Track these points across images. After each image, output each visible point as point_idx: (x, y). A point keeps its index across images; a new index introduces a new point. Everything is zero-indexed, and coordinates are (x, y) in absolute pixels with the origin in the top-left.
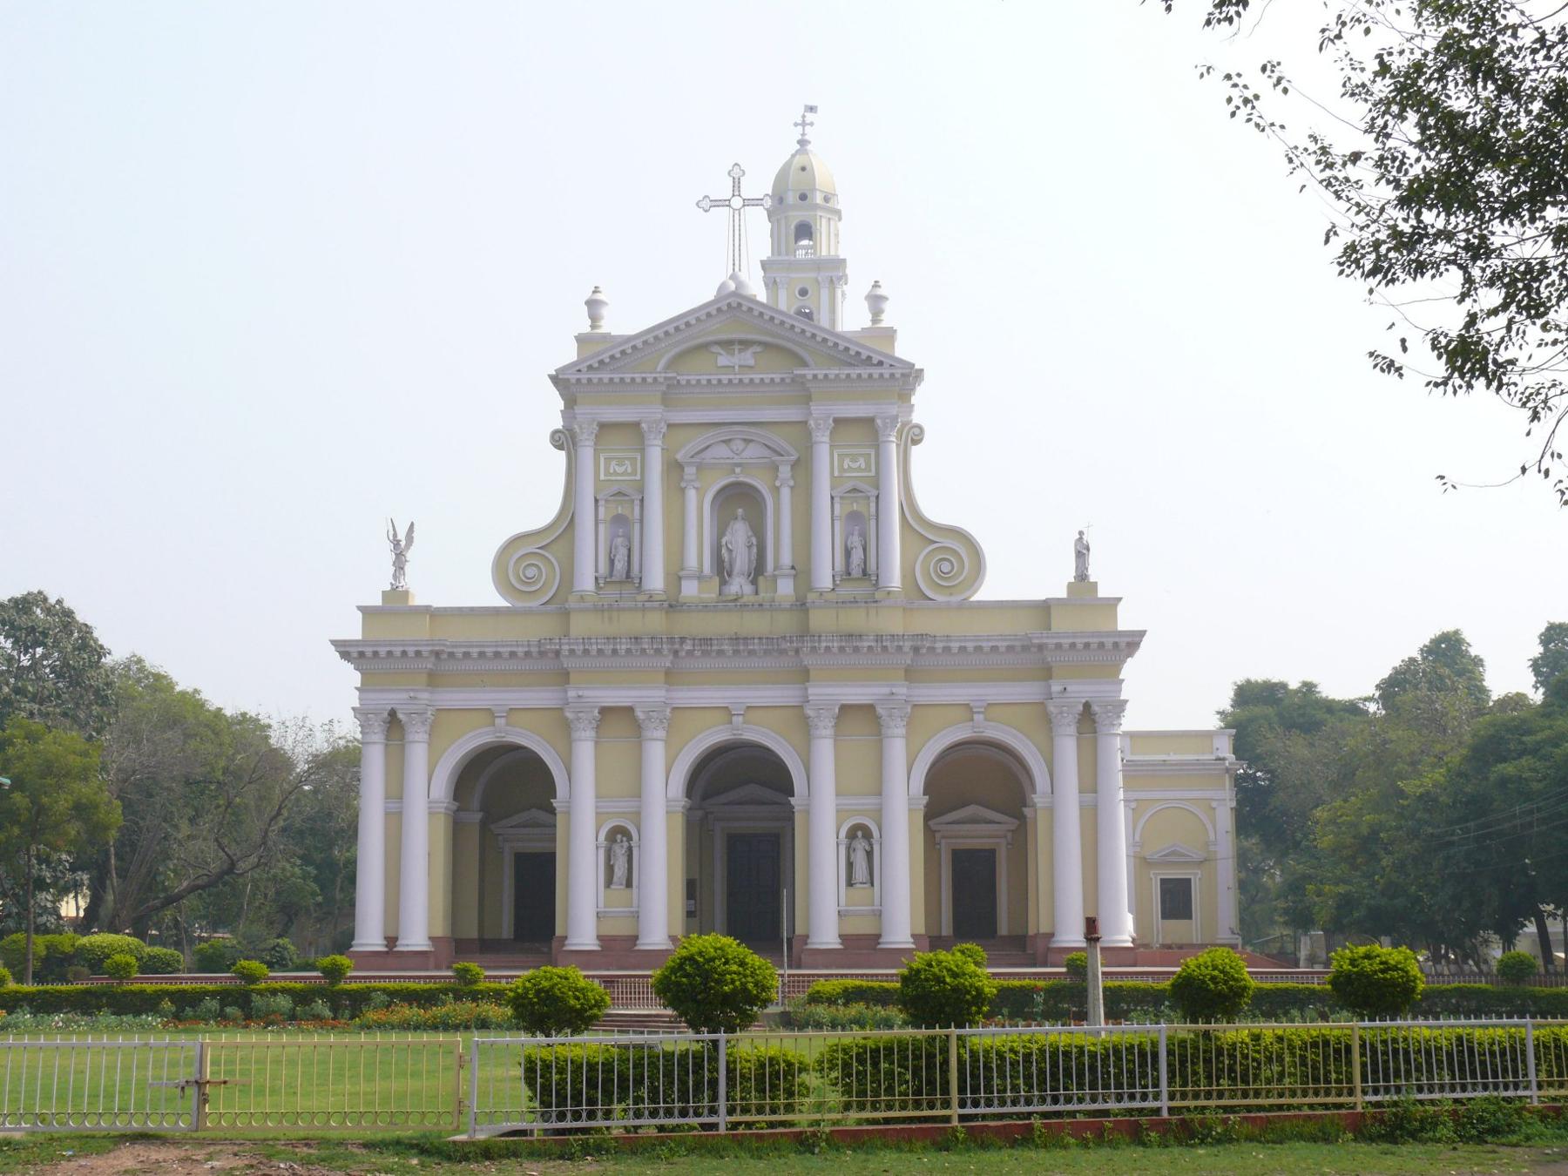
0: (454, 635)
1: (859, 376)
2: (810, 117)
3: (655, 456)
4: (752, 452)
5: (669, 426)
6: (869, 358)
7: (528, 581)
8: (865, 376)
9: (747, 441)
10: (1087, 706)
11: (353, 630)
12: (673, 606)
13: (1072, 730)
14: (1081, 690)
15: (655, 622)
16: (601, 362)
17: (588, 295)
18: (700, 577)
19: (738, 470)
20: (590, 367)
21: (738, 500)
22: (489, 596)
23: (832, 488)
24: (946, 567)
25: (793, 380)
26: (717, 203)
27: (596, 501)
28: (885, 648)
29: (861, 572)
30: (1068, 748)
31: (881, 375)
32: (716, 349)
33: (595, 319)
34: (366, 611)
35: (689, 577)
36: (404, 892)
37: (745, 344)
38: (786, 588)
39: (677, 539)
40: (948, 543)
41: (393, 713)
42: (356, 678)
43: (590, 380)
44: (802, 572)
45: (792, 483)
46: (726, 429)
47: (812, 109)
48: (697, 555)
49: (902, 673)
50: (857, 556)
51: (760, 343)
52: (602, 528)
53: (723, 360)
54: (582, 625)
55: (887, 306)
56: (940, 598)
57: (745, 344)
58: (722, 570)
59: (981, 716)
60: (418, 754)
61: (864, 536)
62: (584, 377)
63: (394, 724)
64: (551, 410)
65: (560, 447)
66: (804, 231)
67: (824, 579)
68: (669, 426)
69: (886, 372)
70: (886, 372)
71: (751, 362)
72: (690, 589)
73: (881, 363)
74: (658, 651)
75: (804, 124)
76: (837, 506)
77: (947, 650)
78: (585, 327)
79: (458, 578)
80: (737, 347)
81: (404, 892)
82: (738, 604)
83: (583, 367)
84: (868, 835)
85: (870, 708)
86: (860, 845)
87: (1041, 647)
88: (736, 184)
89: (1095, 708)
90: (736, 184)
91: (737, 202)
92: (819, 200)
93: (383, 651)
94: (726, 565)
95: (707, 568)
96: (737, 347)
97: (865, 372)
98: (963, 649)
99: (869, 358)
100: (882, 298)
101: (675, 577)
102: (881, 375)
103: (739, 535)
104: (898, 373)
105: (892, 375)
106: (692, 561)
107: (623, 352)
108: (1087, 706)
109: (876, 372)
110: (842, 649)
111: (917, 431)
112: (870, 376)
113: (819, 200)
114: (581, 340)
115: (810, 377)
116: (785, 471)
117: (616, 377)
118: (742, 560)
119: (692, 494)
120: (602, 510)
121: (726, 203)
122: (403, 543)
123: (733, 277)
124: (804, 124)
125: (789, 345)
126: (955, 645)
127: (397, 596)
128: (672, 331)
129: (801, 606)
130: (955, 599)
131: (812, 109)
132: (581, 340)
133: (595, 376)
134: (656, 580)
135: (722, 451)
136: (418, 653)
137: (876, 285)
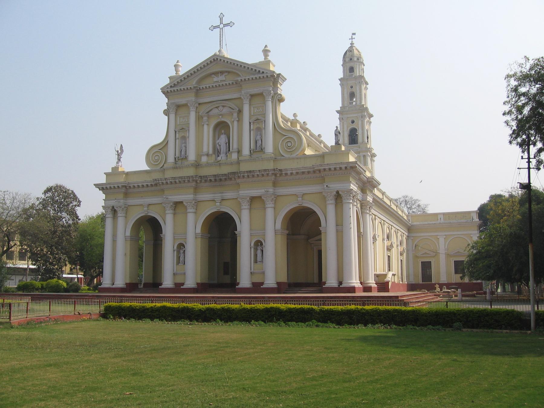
0: (133, 180)
1: (256, 78)
2: (354, 36)
3: (193, 115)
4: (225, 110)
5: (199, 104)
6: (259, 71)
7: (157, 161)
8: (254, 78)
9: (223, 106)
10: (338, 192)
11: (103, 180)
12: (197, 165)
13: (333, 202)
14: (335, 186)
15: (191, 172)
16: (174, 84)
17: (175, 63)
18: (208, 155)
19: (221, 117)
20: (171, 87)
21: (222, 127)
22: (145, 167)
23: (250, 119)
24: (289, 144)
25: (236, 83)
26: (215, 27)
27: (176, 132)
28: (263, 175)
29: (258, 149)
30: (331, 210)
31: (263, 77)
32: (213, 76)
33: (177, 71)
34: (107, 174)
35: (203, 155)
36: (117, 269)
37: (222, 73)
38: (234, 156)
39: (200, 142)
40: (290, 135)
41: (113, 207)
42: (104, 196)
43: (171, 91)
44: (239, 152)
45: (237, 119)
46: (215, 103)
47: (354, 34)
48: (207, 146)
49: (271, 184)
50: (259, 143)
51: (226, 72)
52: (177, 141)
53: (215, 79)
54: (170, 174)
55: (269, 54)
56: (286, 156)
57: (222, 73)
58: (217, 152)
59: (301, 198)
60: (121, 221)
61: (261, 135)
62: (169, 90)
63: (114, 211)
64: (163, 102)
65: (166, 115)
66: (352, 70)
67: (246, 151)
68: (199, 104)
69: (265, 75)
70: (265, 75)
71: (224, 79)
72: (204, 159)
73: (263, 72)
74: (189, 181)
75: (352, 38)
76: (252, 126)
77: (286, 174)
78: (173, 74)
79: (136, 162)
80: (220, 74)
81: (117, 269)
82: (219, 164)
83: (169, 86)
84: (262, 244)
85: (260, 197)
86: (259, 248)
87: (320, 171)
88: (221, 19)
89: (340, 193)
90: (221, 19)
91: (221, 26)
92: (355, 59)
93: (108, 186)
94: (219, 150)
95: (211, 152)
96: (220, 74)
97: (257, 76)
98: (292, 174)
99: (259, 71)
100: (269, 51)
101: (199, 156)
102: (263, 77)
103: (223, 139)
104: (269, 75)
105: (267, 76)
106: (205, 149)
107: (181, 80)
108: (338, 192)
109: (261, 76)
110: (248, 176)
111: (280, 96)
112: (260, 77)
113: (355, 59)
114: (170, 78)
115: (240, 80)
116: (235, 115)
117: (182, 88)
118: (223, 148)
119: (206, 127)
120: (177, 135)
121: (218, 27)
122: (120, 152)
123: (220, 51)
124: (352, 38)
125: (237, 72)
126: (289, 172)
127: (115, 169)
128: (196, 71)
129: (238, 162)
130: (294, 155)
131: (354, 34)
132: (170, 78)
133: (172, 89)
134: (192, 157)
135: (215, 111)
136: (118, 187)
137: (266, 46)
